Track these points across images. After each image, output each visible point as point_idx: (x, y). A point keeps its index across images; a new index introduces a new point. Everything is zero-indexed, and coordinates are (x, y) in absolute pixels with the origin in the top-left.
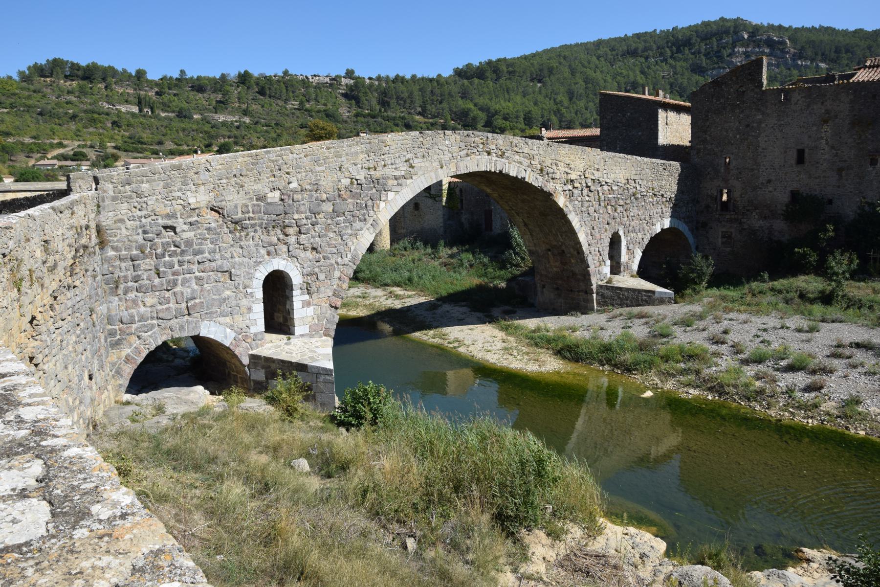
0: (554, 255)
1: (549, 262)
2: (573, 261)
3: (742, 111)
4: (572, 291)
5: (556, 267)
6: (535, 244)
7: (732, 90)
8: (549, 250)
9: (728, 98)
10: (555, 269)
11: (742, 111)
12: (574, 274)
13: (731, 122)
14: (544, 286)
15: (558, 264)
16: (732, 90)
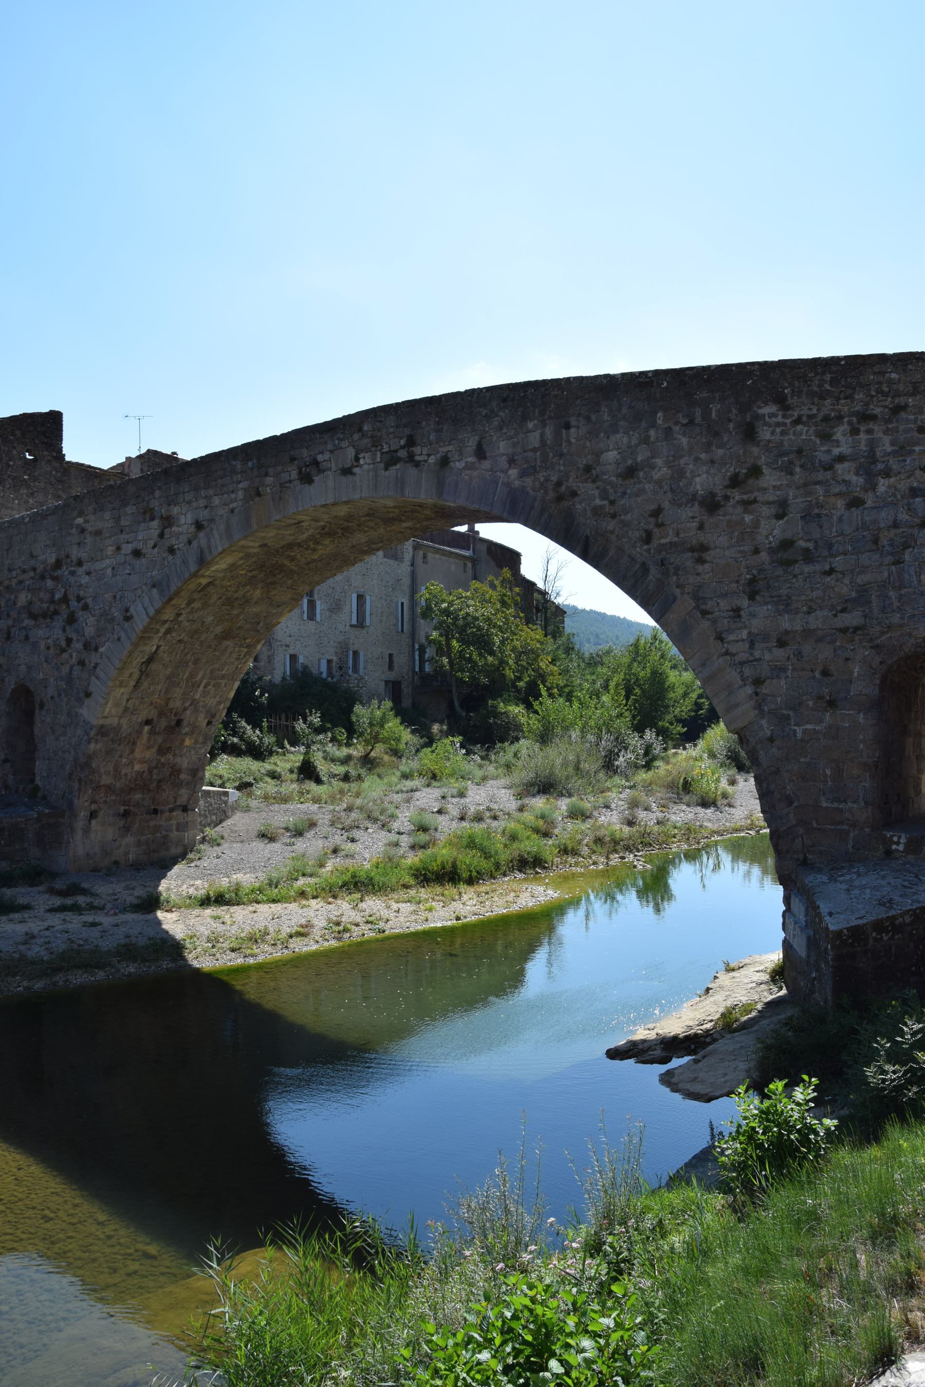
0: (152, 732)
1: (132, 752)
2: (188, 742)
3: (32, 494)
4: (155, 811)
5: (141, 762)
6: (126, 709)
7: (14, 452)
8: (148, 722)
9: (9, 466)
10: (137, 767)
11: (32, 494)
12: (176, 771)
13: (12, 509)
14: (93, 815)
15: (150, 754)
16: (14, 452)
